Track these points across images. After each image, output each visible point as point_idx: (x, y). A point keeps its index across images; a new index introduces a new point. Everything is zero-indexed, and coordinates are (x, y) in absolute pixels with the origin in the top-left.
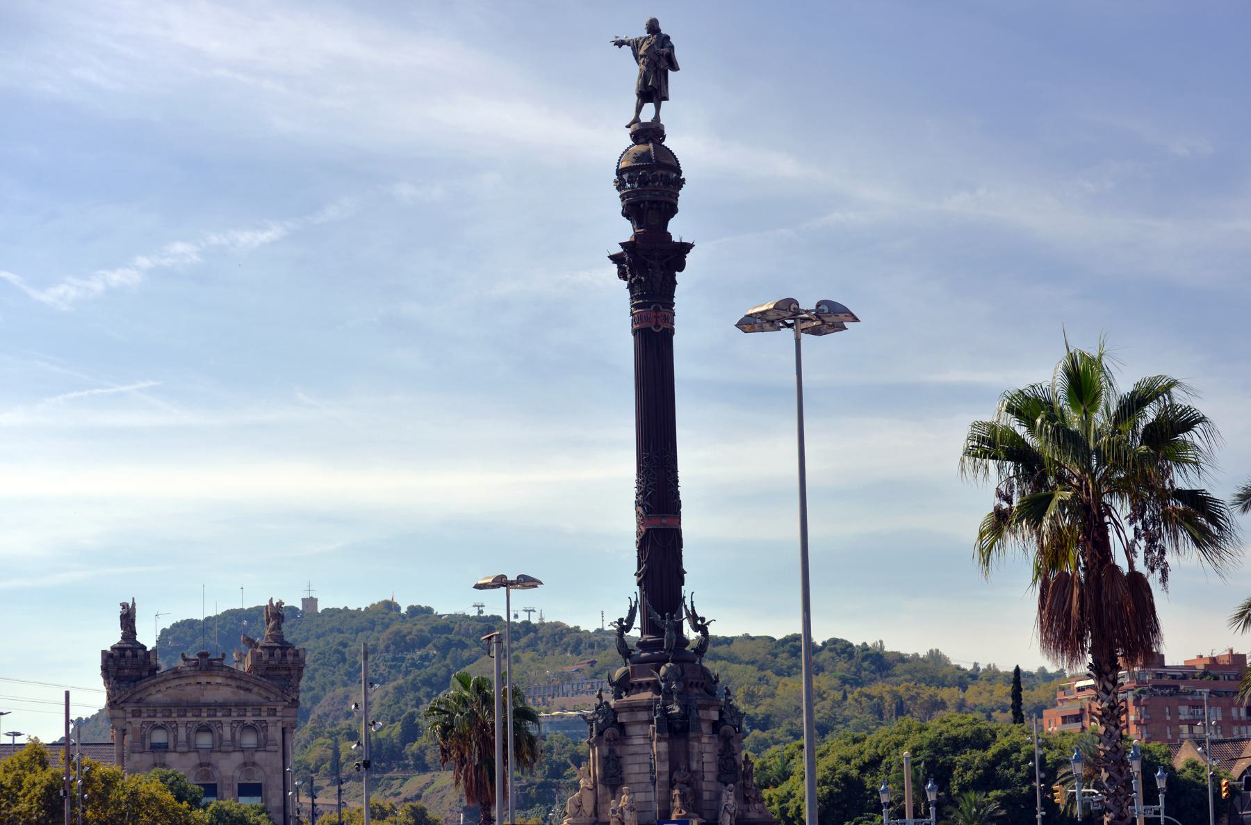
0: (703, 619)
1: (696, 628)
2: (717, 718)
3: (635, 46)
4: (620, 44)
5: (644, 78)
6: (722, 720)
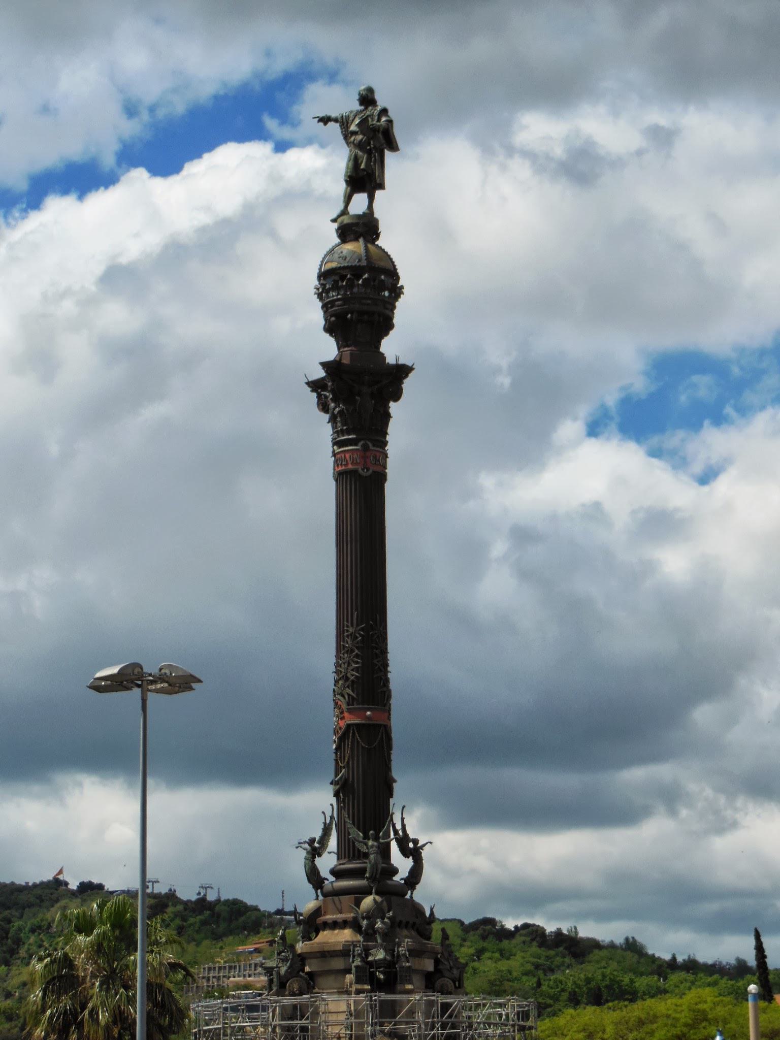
0: (415, 842)
1: (405, 852)
2: (431, 968)
3: (344, 122)
4: (325, 120)
5: (356, 161)
6: (438, 971)
